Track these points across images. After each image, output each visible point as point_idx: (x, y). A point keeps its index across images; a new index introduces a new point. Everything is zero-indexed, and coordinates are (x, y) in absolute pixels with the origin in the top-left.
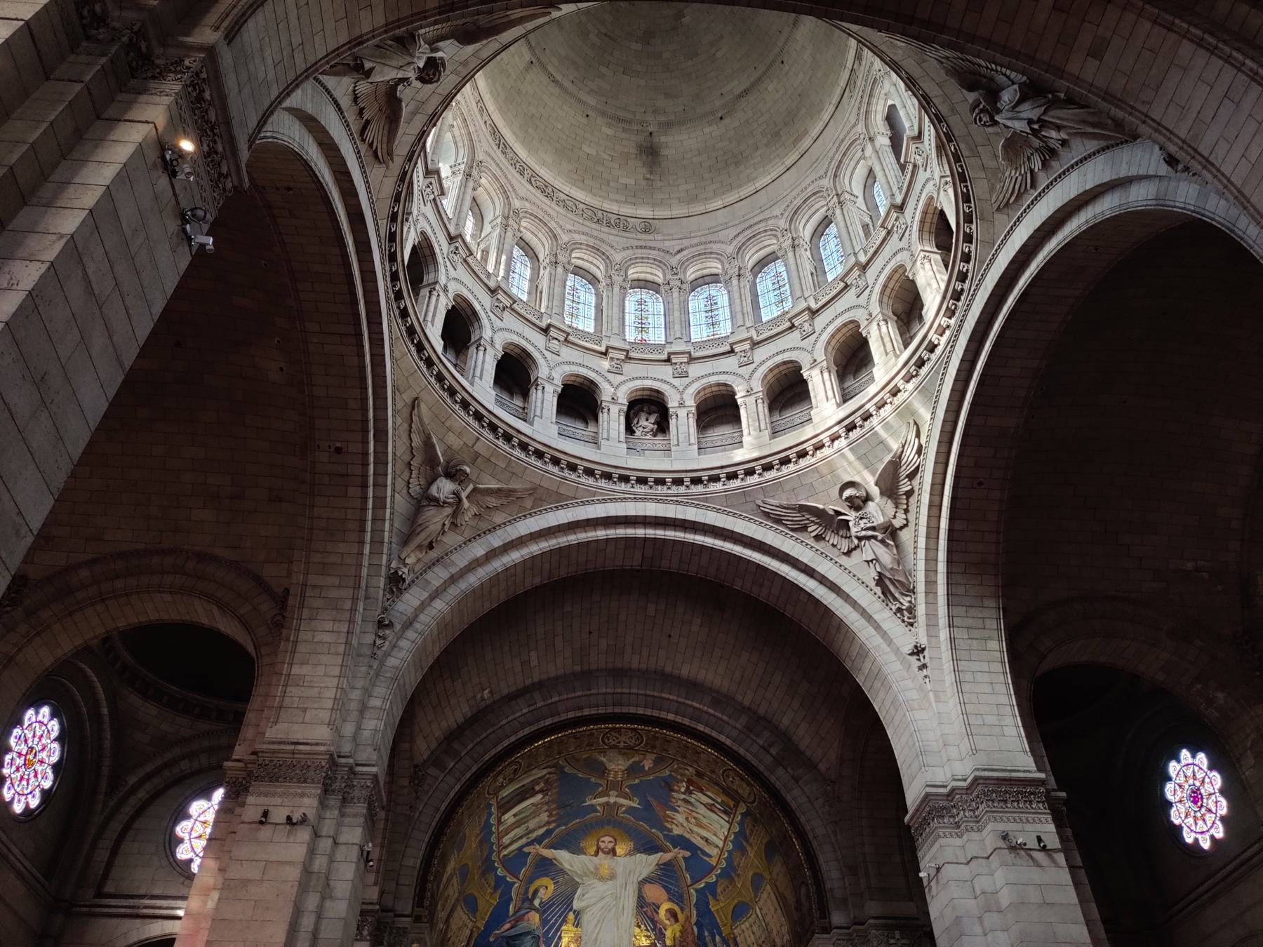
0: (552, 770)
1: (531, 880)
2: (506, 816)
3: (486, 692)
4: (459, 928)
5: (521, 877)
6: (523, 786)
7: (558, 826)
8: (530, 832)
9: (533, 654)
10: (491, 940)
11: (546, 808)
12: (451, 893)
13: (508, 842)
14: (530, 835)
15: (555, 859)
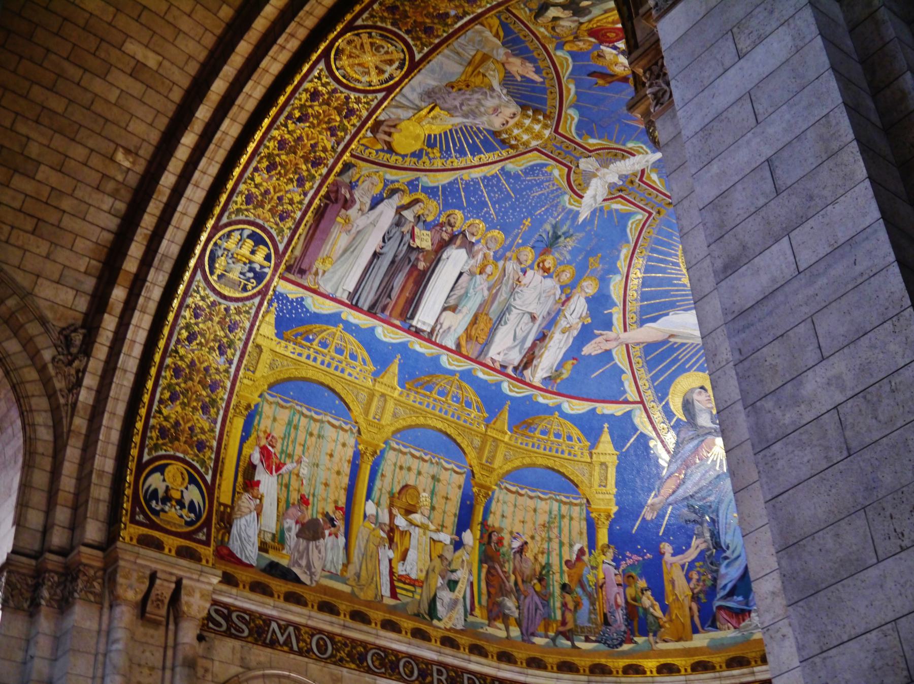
0: (396, 201)
1: (662, 392)
2: (425, 317)
3: (120, 156)
4: (547, 526)
5: (632, 395)
6: (376, 255)
7: (604, 281)
8: (552, 321)
9: (131, 47)
10: (649, 518)
11: (512, 267)
12: (424, 483)
13: (515, 357)
14: (563, 323)
15: (672, 336)
